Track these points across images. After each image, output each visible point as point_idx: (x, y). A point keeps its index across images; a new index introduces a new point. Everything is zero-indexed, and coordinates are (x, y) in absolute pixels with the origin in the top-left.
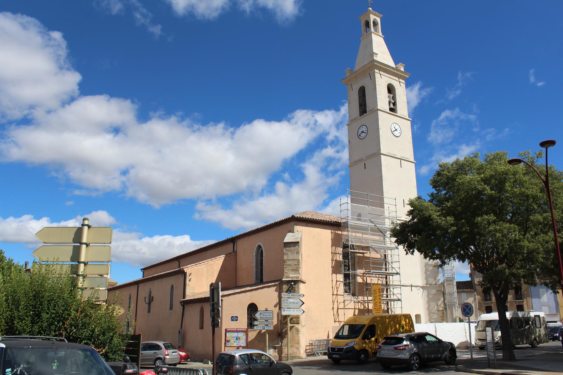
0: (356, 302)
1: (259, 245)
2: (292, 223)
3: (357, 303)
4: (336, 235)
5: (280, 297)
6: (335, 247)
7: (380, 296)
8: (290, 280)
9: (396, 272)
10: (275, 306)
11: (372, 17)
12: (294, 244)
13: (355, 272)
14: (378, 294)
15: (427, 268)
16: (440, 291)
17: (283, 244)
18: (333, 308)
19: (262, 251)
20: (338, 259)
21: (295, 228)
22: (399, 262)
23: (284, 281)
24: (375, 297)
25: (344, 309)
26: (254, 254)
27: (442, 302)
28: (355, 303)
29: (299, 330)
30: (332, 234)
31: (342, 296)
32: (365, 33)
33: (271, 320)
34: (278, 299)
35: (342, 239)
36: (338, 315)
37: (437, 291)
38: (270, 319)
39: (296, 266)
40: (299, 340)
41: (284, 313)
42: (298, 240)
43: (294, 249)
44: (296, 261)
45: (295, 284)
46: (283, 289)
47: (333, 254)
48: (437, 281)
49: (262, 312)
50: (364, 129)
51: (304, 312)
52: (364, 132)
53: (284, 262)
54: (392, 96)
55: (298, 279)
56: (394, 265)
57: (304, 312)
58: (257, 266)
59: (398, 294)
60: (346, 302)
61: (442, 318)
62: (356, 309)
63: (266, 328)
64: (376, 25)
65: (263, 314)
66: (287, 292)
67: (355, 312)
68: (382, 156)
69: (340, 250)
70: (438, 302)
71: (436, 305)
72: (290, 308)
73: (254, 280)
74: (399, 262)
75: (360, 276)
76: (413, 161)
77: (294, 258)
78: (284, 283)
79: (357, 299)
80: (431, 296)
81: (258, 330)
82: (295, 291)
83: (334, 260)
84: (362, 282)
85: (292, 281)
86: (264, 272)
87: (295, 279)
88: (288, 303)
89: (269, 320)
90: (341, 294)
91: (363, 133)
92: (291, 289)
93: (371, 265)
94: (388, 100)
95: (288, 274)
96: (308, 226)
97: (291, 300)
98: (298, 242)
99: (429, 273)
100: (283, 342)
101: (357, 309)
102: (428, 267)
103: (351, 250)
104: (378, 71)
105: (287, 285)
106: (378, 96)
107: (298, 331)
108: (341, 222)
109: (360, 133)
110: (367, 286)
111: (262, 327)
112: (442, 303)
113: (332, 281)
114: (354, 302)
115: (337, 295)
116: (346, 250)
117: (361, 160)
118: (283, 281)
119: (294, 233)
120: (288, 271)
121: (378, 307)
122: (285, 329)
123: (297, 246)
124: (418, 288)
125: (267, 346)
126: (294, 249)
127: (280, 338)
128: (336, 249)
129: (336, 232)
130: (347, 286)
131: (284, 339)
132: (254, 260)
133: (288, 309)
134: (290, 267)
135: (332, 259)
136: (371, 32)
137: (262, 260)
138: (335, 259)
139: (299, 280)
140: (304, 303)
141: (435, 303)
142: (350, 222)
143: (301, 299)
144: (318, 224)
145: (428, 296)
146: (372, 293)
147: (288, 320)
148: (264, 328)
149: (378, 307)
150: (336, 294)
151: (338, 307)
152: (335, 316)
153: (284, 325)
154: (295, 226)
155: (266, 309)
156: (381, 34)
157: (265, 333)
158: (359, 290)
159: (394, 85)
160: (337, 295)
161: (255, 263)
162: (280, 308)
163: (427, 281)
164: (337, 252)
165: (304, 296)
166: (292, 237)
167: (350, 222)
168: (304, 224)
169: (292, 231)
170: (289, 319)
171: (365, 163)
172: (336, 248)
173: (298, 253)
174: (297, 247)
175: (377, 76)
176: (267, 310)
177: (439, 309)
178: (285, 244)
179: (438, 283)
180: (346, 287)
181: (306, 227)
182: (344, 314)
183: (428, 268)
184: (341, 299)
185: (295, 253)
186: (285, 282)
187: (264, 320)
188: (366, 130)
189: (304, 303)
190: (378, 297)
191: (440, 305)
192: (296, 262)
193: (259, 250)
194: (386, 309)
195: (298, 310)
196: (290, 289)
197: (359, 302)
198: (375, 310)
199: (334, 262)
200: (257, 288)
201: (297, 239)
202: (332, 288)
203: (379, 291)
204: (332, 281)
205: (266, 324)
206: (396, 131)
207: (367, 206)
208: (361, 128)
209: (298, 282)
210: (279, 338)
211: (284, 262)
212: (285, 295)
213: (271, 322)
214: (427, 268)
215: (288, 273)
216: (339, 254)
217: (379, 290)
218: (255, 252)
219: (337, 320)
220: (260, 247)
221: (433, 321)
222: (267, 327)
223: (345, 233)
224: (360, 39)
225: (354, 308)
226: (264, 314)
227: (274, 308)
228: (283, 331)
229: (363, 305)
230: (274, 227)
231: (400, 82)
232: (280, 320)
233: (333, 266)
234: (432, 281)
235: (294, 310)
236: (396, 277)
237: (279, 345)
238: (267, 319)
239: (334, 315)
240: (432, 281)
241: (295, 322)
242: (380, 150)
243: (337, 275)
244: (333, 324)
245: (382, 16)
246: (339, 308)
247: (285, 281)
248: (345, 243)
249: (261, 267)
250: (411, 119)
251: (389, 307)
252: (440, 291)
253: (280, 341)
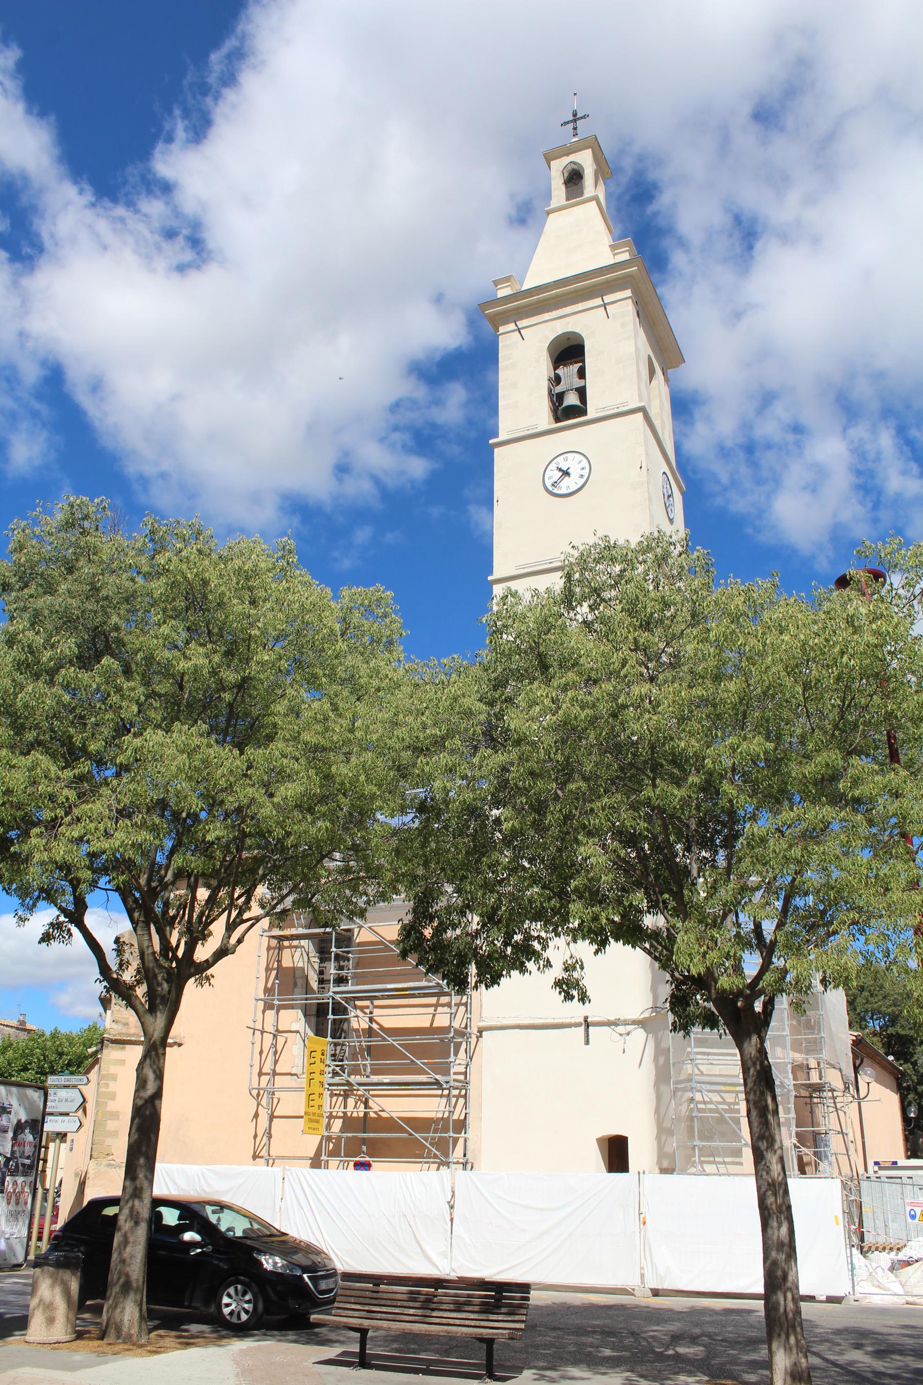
13: (306, 999)
18: (256, 1115)
62: (337, 1117)
83: (273, 969)
90: (289, 1071)
101: (340, 1117)
124: (621, 1029)
160: (275, 1073)
199: (274, 973)
233: (269, 985)
239: (255, 1136)
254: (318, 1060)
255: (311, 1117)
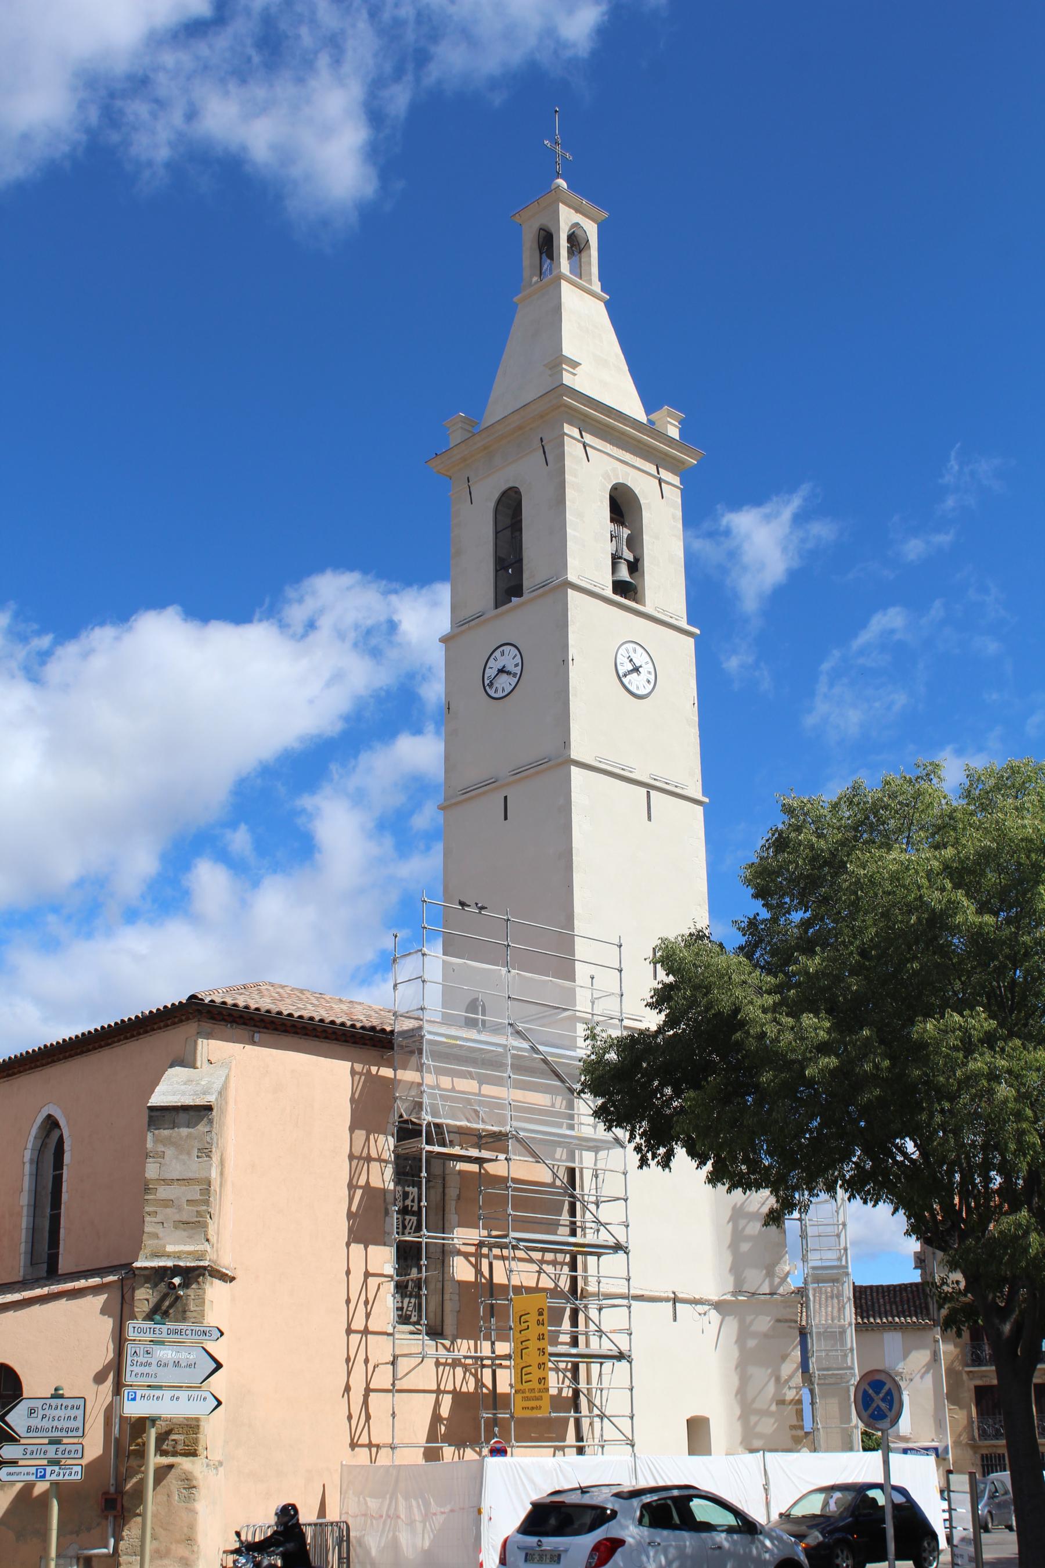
0: (445, 1364)
1: (49, 1116)
2: (190, 1028)
3: (447, 1368)
4: (373, 1081)
5: (120, 1340)
6: (364, 1132)
7: (541, 1337)
8: (165, 1269)
9: (611, 1241)
10: (99, 1378)
11: (567, 218)
12: (192, 1113)
13: (443, 1239)
14: (535, 1330)
15: (740, 1228)
16: (786, 1321)
17: (147, 1111)
18: (348, 1389)
19: (61, 1141)
20: (376, 1182)
21: (199, 1047)
22: (626, 1200)
23: (140, 1268)
24: (522, 1342)
25: (393, 1390)
26: (28, 1155)
27: (795, 1366)
28: (441, 1368)
29: (195, 1483)
30: (357, 1077)
31: (386, 1337)
32: (535, 279)
33: (75, 1440)
34: (111, 1346)
35: (395, 1099)
36: (368, 1417)
37: (778, 1321)
38: (70, 1434)
39: (195, 1209)
40: (192, 1527)
41: (134, 1409)
42: (211, 1099)
43: (190, 1133)
44: (198, 1188)
45: (185, 1285)
46: (136, 1303)
47: (355, 1162)
48: (777, 1280)
49: (38, 1404)
50: (508, 659)
51: (219, 1403)
52: (509, 673)
53: (147, 1190)
54: (626, 532)
55: (202, 1264)
56: (608, 1213)
57: (219, 1403)
58: (36, 1206)
59: (620, 1331)
60: (404, 1365)
61: (794, 1432)
63: (55, 1474)
64: (580, 252)
65: (41, 1413)
66: (149, 1317)
67: (437, 1404)
68: (574, 770)
69: (385, 1145)
70: (779, 1370)
71: (773, 1380)
72: (159, 1387)
73: (22, 1264)
74: (626, 1200)
75: (466, 1255)
76: (698, 795)
77: (190, 1175)
78: (142, 1280)
79: (448, 1350)
80: (751, 1343)
81: (19, 1485)
82: (185, 1312)
83: (357, 1187)
84: (473, 1279)
85: (176, 1270)
86: (62, 1231)
87: (188, 1264)
88: (150, 1364)
89: (65, 1441)
91: (504, 677)
92: (170, 1306)
93: (510, 1211)
94: (609, 548)
95: (161, 1242)
96: (253, 1043)
97: (165, 1353)
98: (209, 1108)
99: (745, 1247)
100: (124, 1534)
101: (448, 1392)
102: (742, 1222)
103: (429, 1148)
104: (575, 432)
105: (155, 1286)
106: (569, 531)
107: (189, 1485)
108: (392, 1032)
109: (490, 673)
110: (492, 1296)
111: (33, 1470)
112: (796, 1370)
113: (348, 1272)
114: (438, 1364)
115: (366, 1332)
116: (410, 1145)
117: (490, 784)
118: (137, 1272)
119: (195, 1067)
120: (159, 1230)
121: (535, 1384)
122: (134, 1480)
123: (203, 1123)
124: (701, 1308)
125: (53, 1553)
126: (189, 1136)
127: (111, 1519)
128: (368, 1139)
129: (374, 1070)
130: (410, 1296)
131: (128, 1522)
132: (26, 1179)
133: (152, 1392)
134: (169, 1210)
135: (351, 1180)
136: (560, 277)
137: (58, 1181)
138: (362, 1182)
139: (205, 1268)
140: (219, 1366)
141: (769, 1371)
142: (430, 1033)
143: (211, 1347)
144: (296, 1033)
145: (741, 1340)
146: (511, 1328)
147: (148, 1438)
148: (44, 1476)
149: (535, 1384)
150: (362, 1328)
151: (368, 1384)
152: (354, 1422)
153: (133, 1462)
154: (200, 1041)
155: (56, 1389)
156: (597, 286)
157: (45, 1496)
158: (459, 1311)
159: (636, 492)
160: (366, 1332)
161: (29, 1191)
162: (118, 1387)
163: (739, 1281)
164: (374, 1154)
165: (222, 1334)
166: (185, 1084)
167: (430, 1033)
168: (240, 1031)
169: (187, 1061)
170: (153, 1433)
171: (506, 798)
172: (372, 1137)
173: (206, 1152)
174: (202, 1128)
175: (572, 449)
176: (62, 1397)
177: (785, 1394)
178: (154, 1114)
179: (781, 1290)
180: (406, 1300)
181: (249, 1048)
182: (393, 1415)
183: (744, 1228)
184: (380, 1349)
185: (195, 1152)
186: (146, 1272)
187: (46, 1441)
188: (516, 665)
189: (219, 1366)
190: (533, 1345)
191: (787, 1381)
192: (194, 1192)
193: (48, 1136)
194: (570, 1394)
195: (195, 1393)
196: (167, 1303)
197: (456, 1363)
198: (520, 1396)
200: (24, 1300)
201: (204, 1094)
202: (348, 1301)
203: (541, 1318)
204: (348, 1272)
205: (51, 1454)
206: (635, 675)
207: (504, 970)
208: (497, 653)
209: (199, 1276)
210: (106, 1518)
211: (147, 1190)
212: (141, 1331)
213: (73, 1448)
214: (740, 1228)
215: (160, 1235)
216: (380, 1160)
217: (541, 1314)
218: (30, 1146)
219: (364, 1440)
220: (51, 1124)
221: (757, 1443)
222: (56, 1468)
223: (408, 1076)
224: (516, 299)
225: (435, 1387)
226: (48, 1412)
227: (94, 1387)
228: (128, 1486)
229: (475, 1375)
230: (114, 1042)
231: (660, 481)
232: (117, 1440)
233: (354, 1209)
234: (756, 1280)
235: (177, 1393)
236: (612, 1263)
237: (105, 1551)
238: (59, 1434)
239: (350, 1417)
240: (756, 1280)
241: (180, 1447)
242: (566, 744)
243: (371, 1248)
244: (347, 1456)
245: (605, 215)
246: (372, 1386)
247: (146, 1268)
248: (405, 1117)
249: (52, 1210)
250: (697, 631)
251: (583, 1385)
252: (786, 1321)
253: (110, 1531)
254: (533, 1323)
255: (527, 1394)
